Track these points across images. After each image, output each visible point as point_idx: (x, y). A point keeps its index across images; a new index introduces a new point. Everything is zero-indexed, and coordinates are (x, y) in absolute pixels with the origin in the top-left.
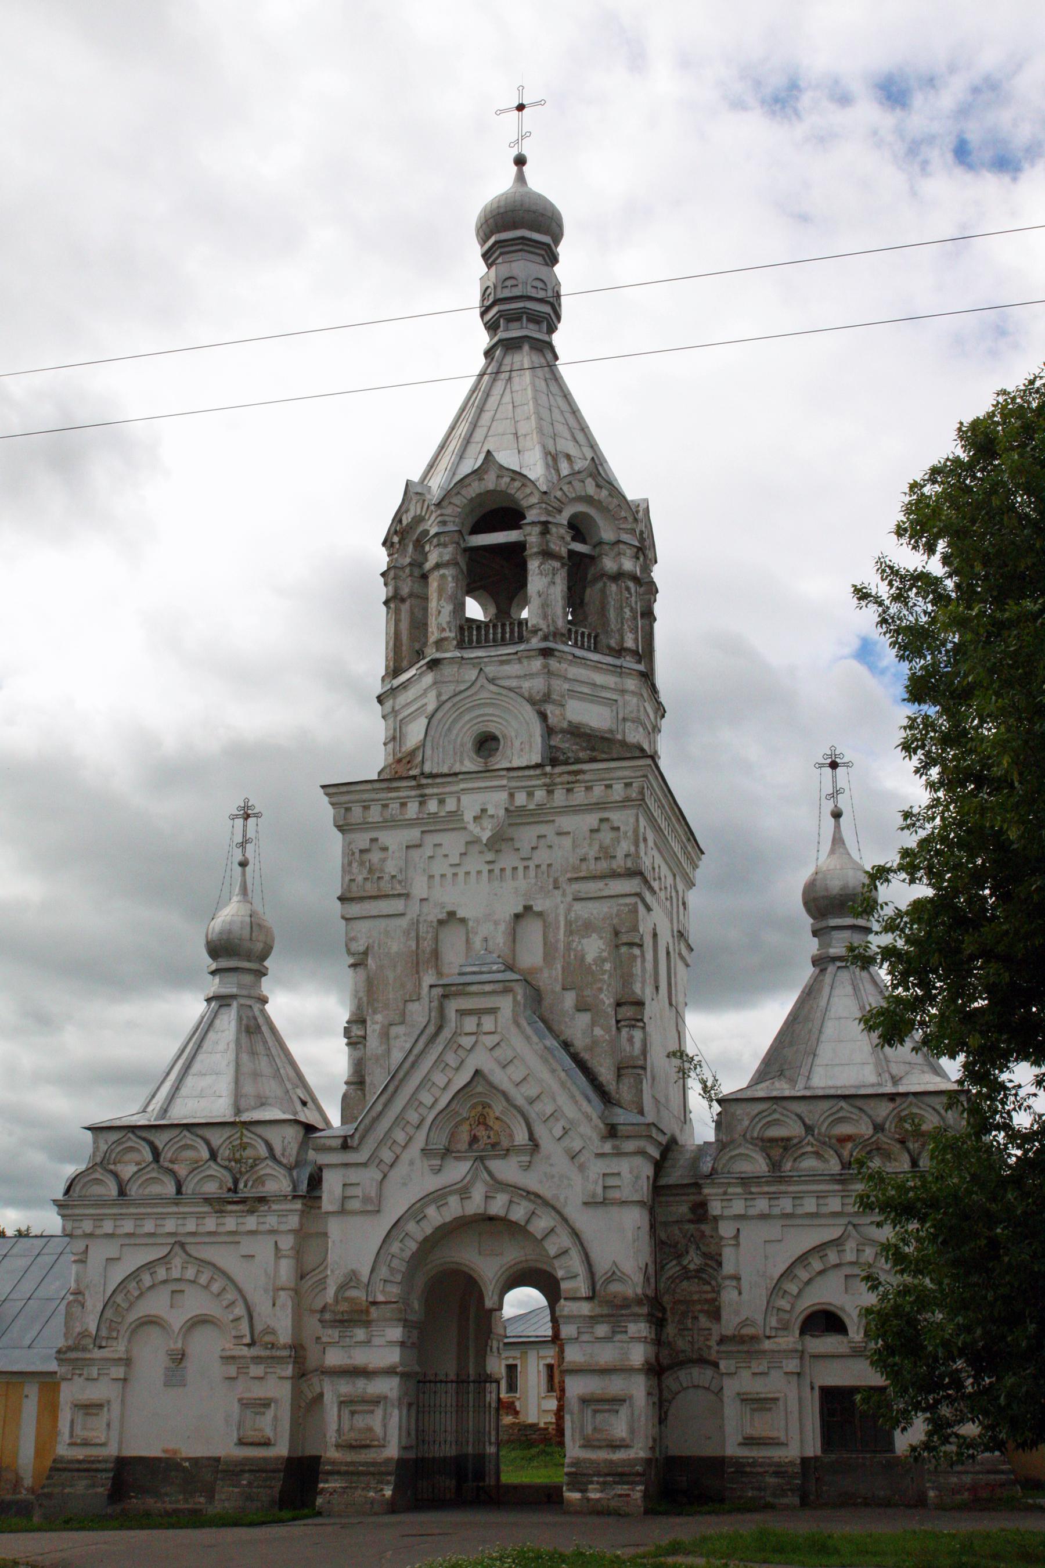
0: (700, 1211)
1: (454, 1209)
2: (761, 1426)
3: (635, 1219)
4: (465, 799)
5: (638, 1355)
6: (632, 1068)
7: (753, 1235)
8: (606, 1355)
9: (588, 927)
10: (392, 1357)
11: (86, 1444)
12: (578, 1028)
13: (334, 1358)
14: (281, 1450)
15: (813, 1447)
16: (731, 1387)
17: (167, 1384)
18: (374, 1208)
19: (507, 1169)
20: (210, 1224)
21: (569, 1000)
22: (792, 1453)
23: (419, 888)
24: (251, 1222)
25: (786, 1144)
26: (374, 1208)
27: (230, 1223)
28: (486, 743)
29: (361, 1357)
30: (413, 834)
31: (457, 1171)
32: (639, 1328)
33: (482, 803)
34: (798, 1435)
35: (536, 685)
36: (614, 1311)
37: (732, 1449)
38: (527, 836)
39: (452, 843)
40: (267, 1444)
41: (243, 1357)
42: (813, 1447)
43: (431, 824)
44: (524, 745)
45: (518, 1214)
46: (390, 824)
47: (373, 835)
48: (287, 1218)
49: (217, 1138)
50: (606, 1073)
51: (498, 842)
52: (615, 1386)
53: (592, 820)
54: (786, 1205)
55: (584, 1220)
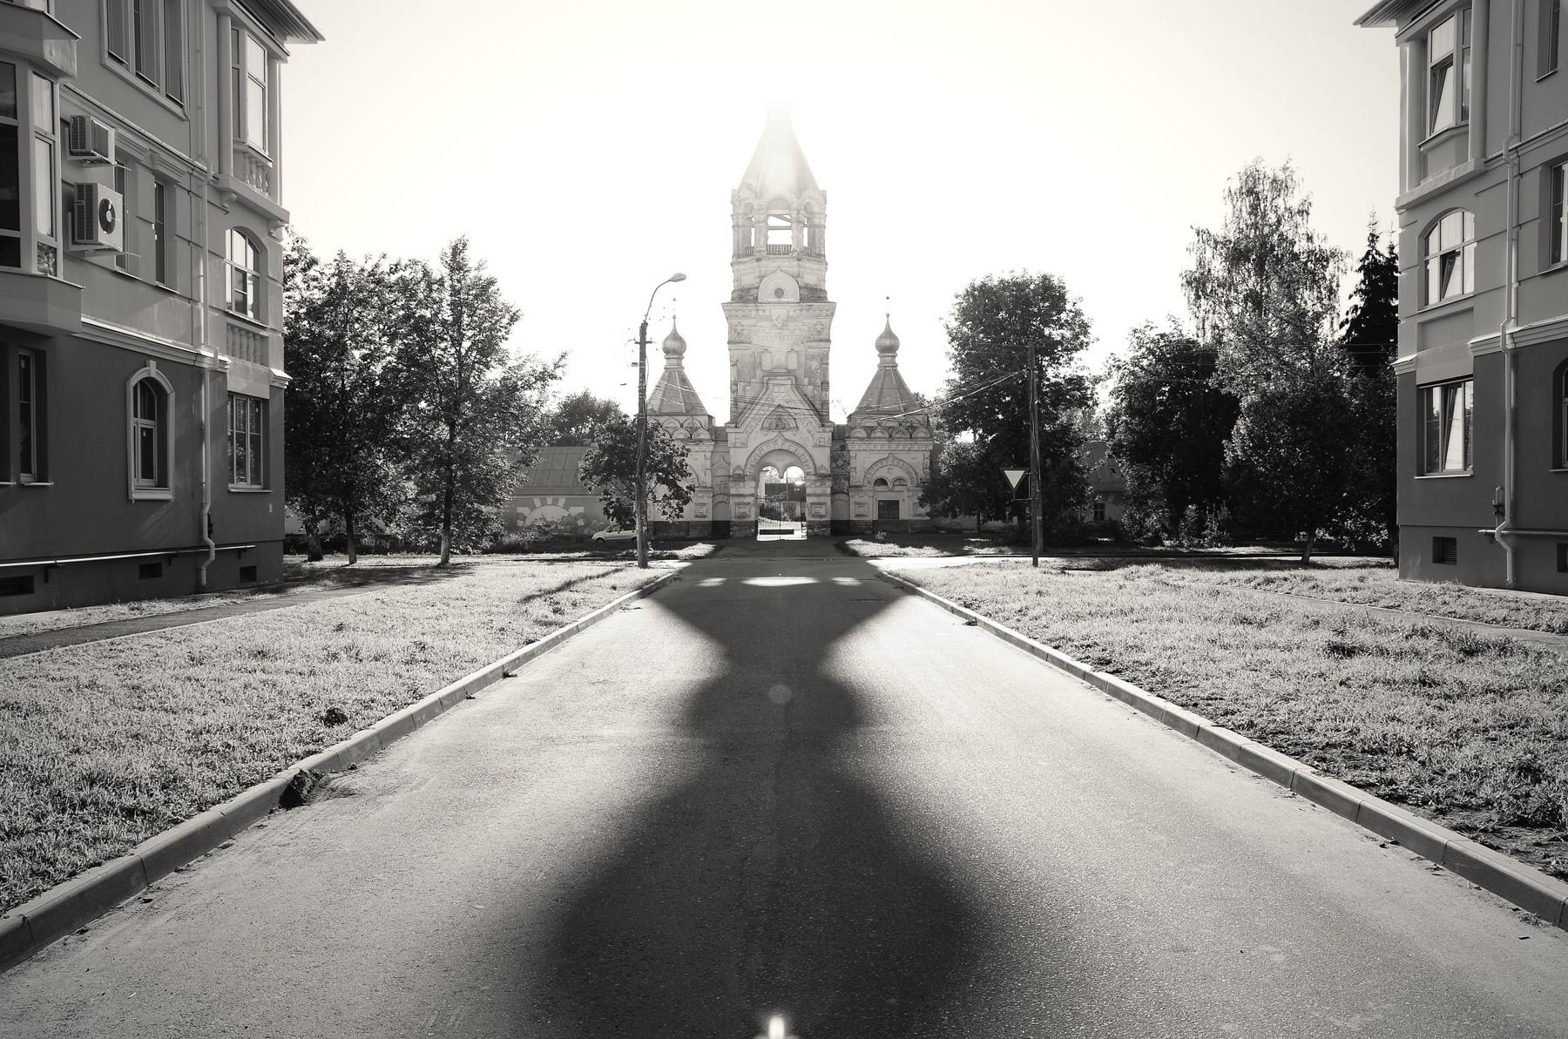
0: (843, 448)
1: (772, 447)
2: (861, 511)
3: (828, 450)
5: (829, 491)
6: (825, 403)
7: (860, 455)
8: (819, 491)
9: (813, 358)
12: (809, 390)
13: (733, 491)
14: (709, 518)
15: (876, 518)
16: (852, 500)
18: (744, 445)
19: (788, 435)
21: (806, 381)
22: (870, 518)
23: (755, 341)
25: (872, 429)
26: (744, 445)
29: (741, 491)
32: (829, 484)
33: (779, 312)
34: (872, 514)
35: (795, 271)
36: (822, 477)
37: (852, 518)
38: (792, 325)
39: (767, 324)
42: (876, 518)
44: (792, 293)
45: (792, 449)
48: (709, 446)
49: (682, 419)
50: (818, 407)
51: (784, 326)
52: (822, 499)
55: (814, 452)
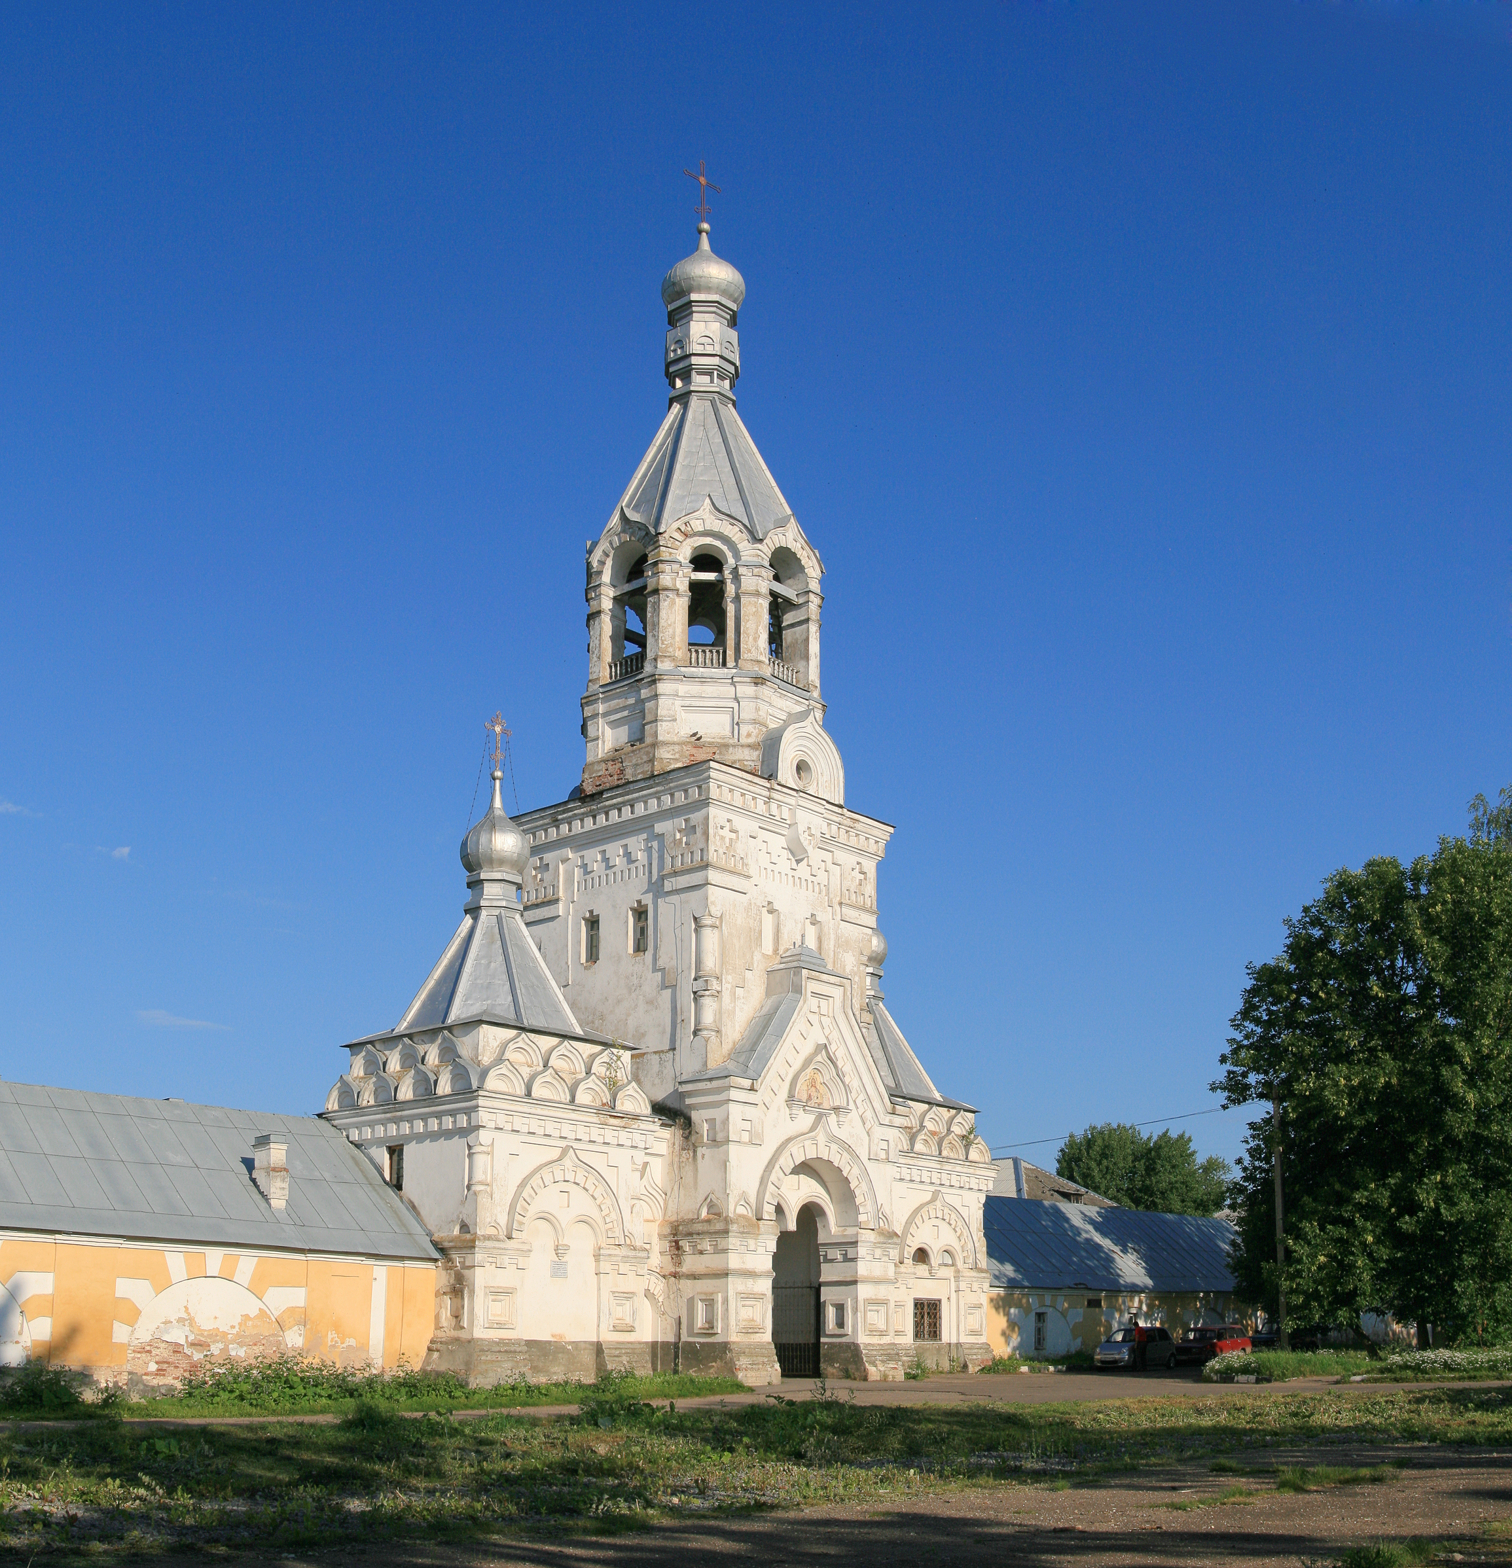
4: (800, 813)
10: (767, 1263)
11: (500, 1326)
17: (554, 1275)
20: (595, 1133)
24: (624, 1137)
27: (609, 1135)
28: (801, 768)
40: (631, 1330)
41: (616, 1255)
43: (769, 822)
46: (744, 811)
47: (731, 817)
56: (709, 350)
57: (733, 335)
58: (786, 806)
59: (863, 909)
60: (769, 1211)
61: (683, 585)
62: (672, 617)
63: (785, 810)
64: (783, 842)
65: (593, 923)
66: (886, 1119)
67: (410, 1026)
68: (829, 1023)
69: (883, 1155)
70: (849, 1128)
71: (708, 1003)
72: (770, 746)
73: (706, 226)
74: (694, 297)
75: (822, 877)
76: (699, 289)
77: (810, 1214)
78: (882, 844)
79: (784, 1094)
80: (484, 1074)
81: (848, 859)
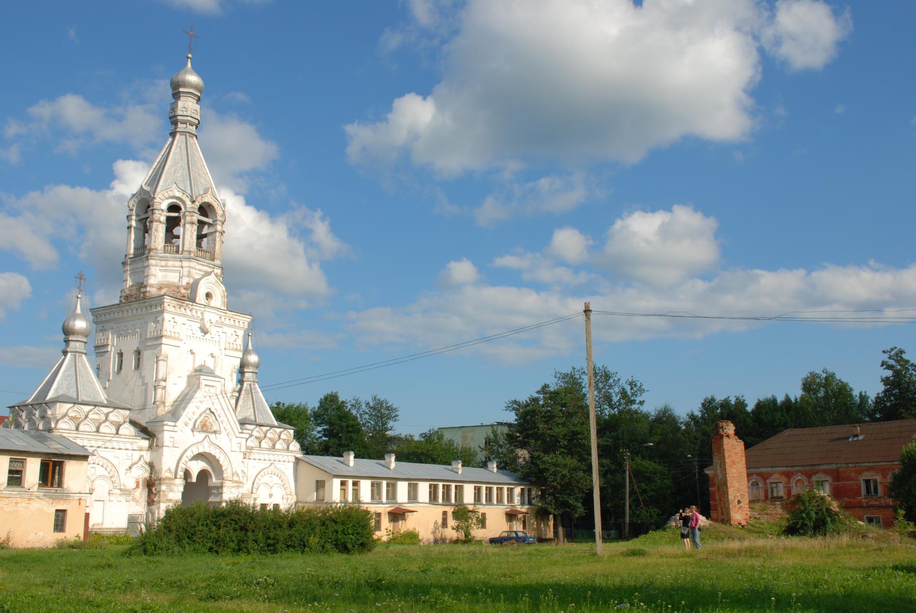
28: (208, 296)
30: (184, 320)
31: (200, 436)
53: (232, 330)
54: (262, 457)
56: (185, 113)
57: (198, 107)
58: (197, 310)
59: (236, 350)
60: (181, 474)
61: (163, 219)
62: (159, 232)
63: (199, 313)
64: (198, 325)
65: (121, 355)
66: (238, 435)
67: (33, 400)
68: (215, 397)
69: (238, 449)
70: (222, 440)
71: (159, 391)
72: (193, 287)
73: (190, 56)
74: (181, 90)
75: (217, 338)
76: (184, 86)
77: (203, 475)
78: (246, 324)
79: (191, 426)
80: (57, 422)
81: (230, 331)
